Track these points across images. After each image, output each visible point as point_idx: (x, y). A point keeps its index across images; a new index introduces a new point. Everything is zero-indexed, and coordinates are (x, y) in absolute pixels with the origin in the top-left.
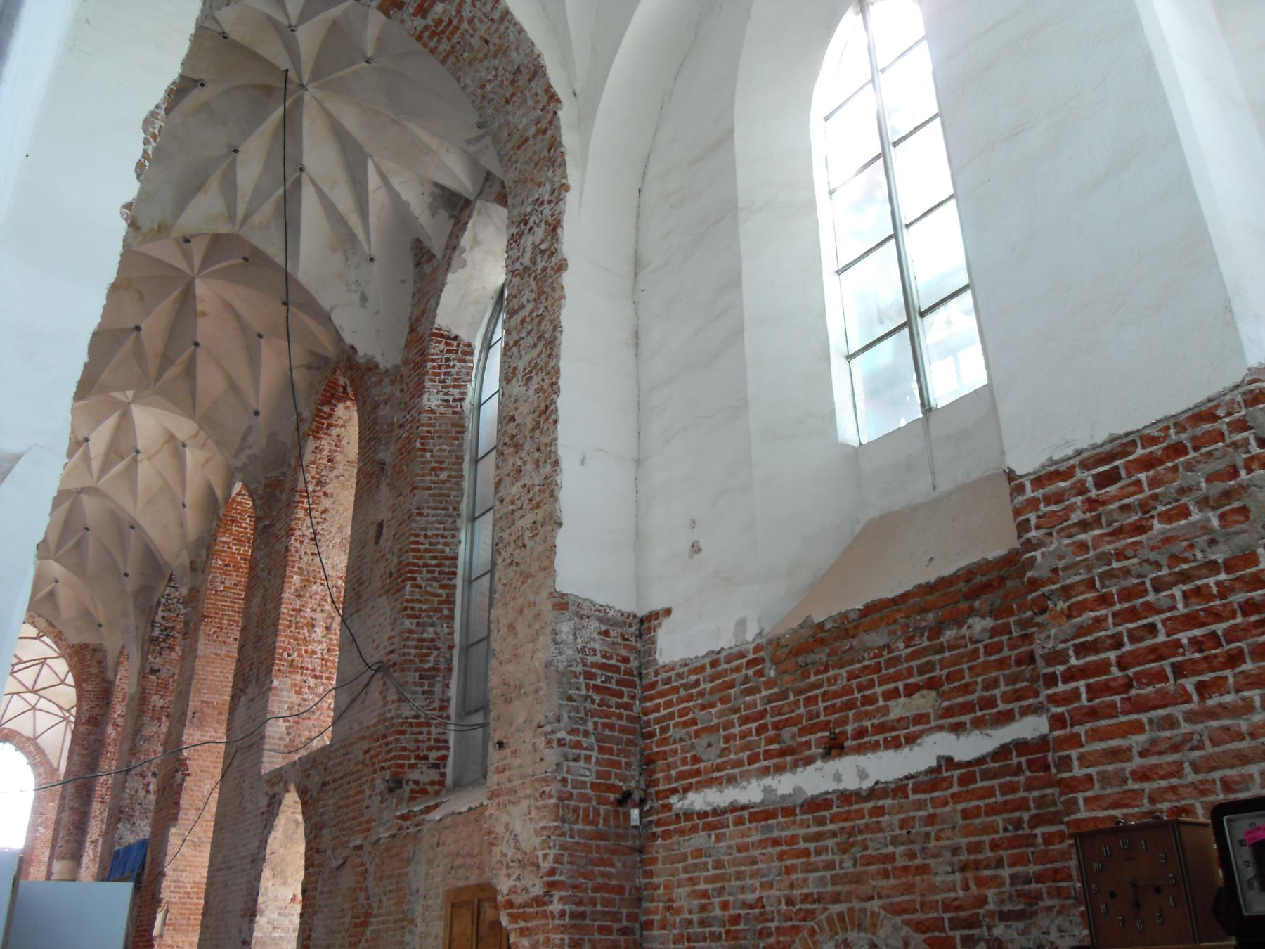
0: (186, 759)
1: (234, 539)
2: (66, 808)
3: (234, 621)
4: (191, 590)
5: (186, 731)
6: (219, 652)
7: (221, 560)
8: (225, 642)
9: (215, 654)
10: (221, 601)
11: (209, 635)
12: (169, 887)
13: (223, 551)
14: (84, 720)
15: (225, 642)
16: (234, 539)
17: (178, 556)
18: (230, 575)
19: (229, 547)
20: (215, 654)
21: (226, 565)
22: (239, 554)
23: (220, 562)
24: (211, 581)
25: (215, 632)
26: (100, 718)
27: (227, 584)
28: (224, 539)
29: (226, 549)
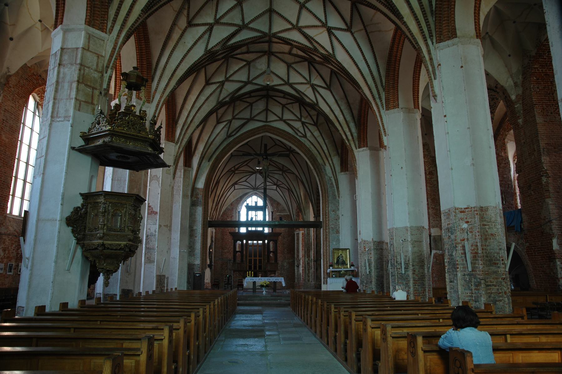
0: (546, 170)
1: (540, 66)
2: (430, 208)
3: (548, 105)
4: (517, 96)
5: (542, 158)
6: (546, 120)
7: (535, 77)
8: (547, 115)
9: (545, 121)
10: (540, 96)
11: (539, 113)
12: (556, 228)
13: (536, 72)
14: (427, 173)
15: (547, 115)
16: (540, 66)
17: (507, 81)
18: (540, 84)
19: (538, 70)
20: (545, 121)
21: (538, 79)
22: (543, 72)
23: (535, 78)
24: (533, 88)
25: (541, 111)
26: (433, 172)
27: (540, 88)
28: (536, 66)
29: (536, 71)
